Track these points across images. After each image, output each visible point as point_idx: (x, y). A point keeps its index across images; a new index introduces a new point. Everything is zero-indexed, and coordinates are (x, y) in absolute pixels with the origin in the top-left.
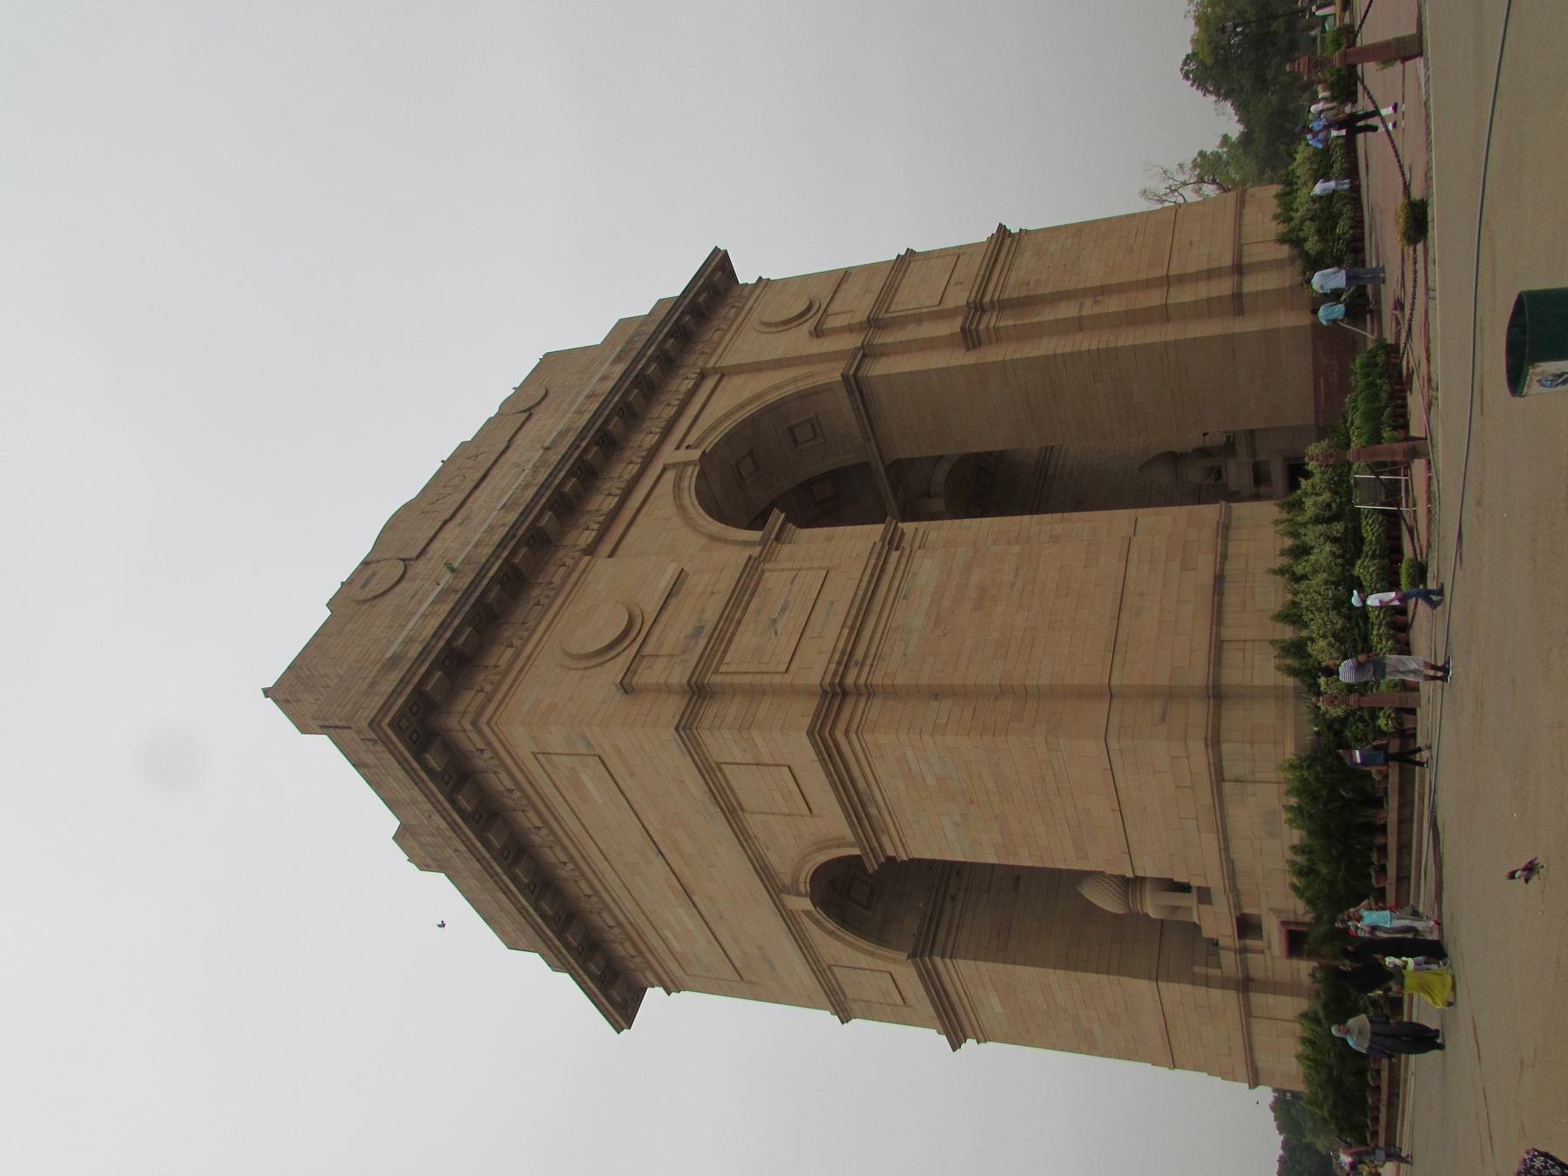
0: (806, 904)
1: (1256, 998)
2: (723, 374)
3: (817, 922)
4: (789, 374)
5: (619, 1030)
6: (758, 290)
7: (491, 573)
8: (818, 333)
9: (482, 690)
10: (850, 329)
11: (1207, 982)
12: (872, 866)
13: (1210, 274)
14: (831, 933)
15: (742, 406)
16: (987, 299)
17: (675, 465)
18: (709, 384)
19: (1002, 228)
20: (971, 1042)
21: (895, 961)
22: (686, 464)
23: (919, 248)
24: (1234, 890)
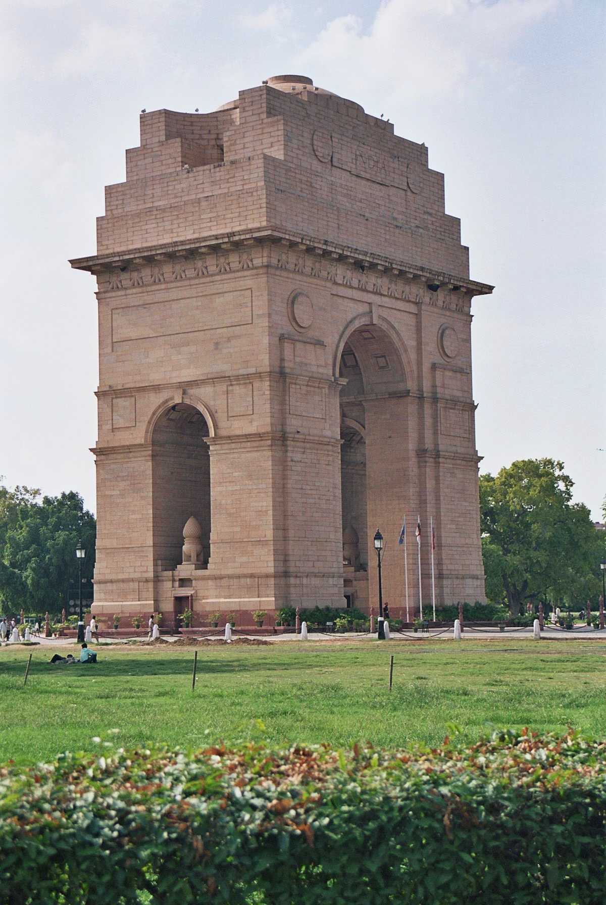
0: (178, 400)
2: (418, 316)
3: (166, 401)
4: (413, 356)
5: (72, 262)
8: (434, 367)
10: (434, 386)
11: (155, 565)
12: (205, 439)
16: (441, 460)
18: (413, 309)
19: (482, 458)
20: (94, 457)
21: (147, 432)
22: (372, 317)
24: (204, 578)
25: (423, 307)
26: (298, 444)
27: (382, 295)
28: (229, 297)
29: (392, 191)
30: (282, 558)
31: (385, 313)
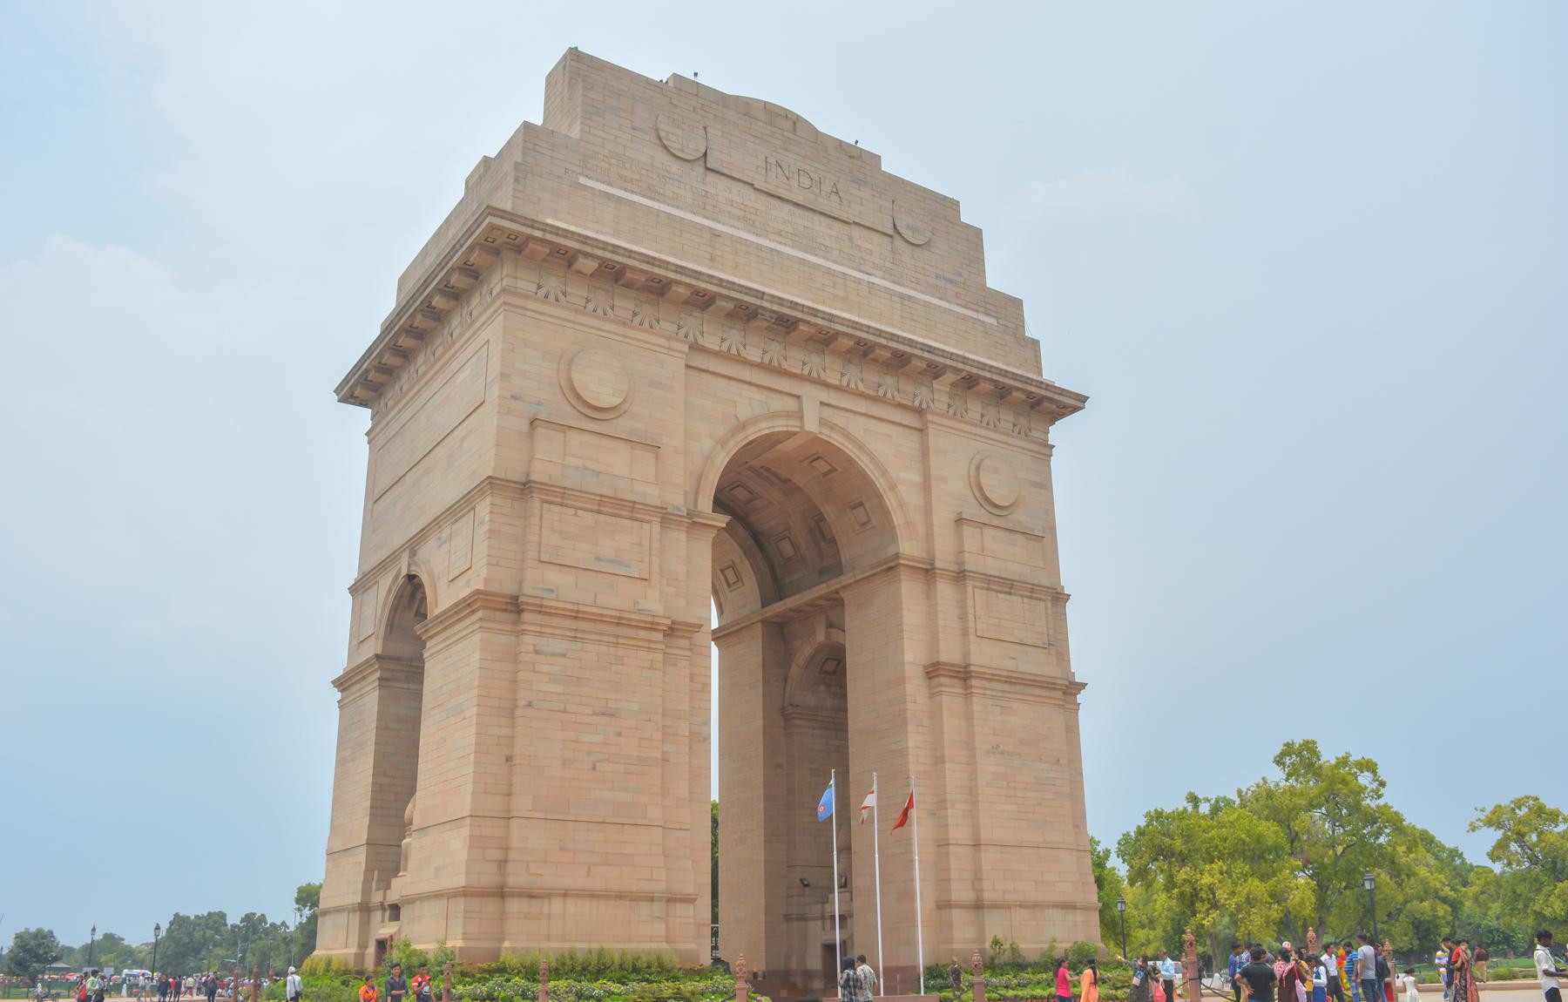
0: (404, 572)
1: (356, 917)
3: (396, 578)
4: (913, 498)
6: (1035, 447)
7: (656, 270)
8: (959, 521)
9: (539, 287)
11: (367, 881)
12: (419, 629)
13: (977, 879)
14: (390, 589)
15: (872, 458)
17: (801, 410)
19: (1084, 685)
20: (339, 696)
22: (802, 418)
23: (1070, 607)
25: (930, 417)
26: (557, 621)
27: (826, 385)
28: (467, 372)
29: (857, 232)
30: (496, 854)
31: (839, 419)
